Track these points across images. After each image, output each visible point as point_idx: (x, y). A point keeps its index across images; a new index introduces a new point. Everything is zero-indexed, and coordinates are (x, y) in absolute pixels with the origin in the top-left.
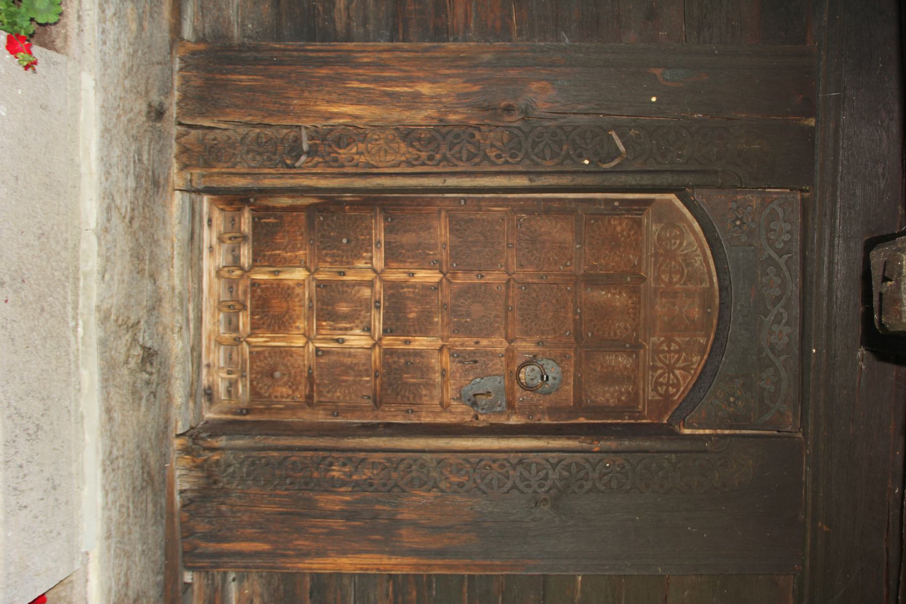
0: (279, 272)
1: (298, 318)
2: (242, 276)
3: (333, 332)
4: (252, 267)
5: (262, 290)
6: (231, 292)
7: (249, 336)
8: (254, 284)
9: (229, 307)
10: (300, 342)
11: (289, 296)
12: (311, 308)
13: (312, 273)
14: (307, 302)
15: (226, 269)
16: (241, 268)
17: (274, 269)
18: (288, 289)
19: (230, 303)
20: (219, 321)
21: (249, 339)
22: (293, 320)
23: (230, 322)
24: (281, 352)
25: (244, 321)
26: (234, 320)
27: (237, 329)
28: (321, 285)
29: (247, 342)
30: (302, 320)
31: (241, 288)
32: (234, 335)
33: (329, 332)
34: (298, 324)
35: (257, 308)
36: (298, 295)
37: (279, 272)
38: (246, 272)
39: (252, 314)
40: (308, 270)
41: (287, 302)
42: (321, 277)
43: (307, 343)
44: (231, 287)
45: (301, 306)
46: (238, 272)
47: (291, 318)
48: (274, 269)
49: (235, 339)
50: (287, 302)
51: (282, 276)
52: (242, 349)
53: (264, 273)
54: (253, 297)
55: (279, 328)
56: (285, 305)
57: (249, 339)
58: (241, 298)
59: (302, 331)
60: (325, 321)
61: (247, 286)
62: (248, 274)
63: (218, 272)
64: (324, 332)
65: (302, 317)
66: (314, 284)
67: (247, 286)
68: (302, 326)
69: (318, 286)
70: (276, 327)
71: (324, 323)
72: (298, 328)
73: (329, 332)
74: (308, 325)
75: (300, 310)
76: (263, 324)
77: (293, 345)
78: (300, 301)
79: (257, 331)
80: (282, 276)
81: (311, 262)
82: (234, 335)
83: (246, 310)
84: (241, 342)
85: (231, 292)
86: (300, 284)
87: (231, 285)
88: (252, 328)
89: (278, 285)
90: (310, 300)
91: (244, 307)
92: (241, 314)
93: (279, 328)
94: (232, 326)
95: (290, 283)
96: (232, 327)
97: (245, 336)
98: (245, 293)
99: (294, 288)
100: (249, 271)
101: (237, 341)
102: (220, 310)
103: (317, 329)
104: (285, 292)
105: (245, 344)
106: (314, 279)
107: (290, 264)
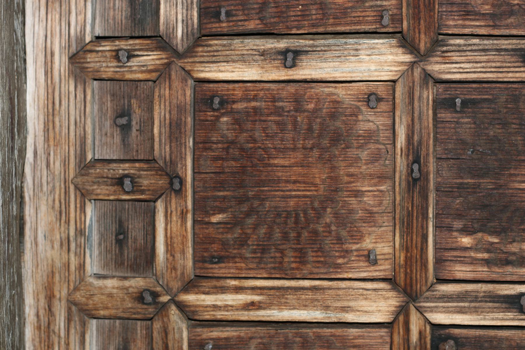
0: (297, 53)
1: (370, 217)
2: (163, 73)
3: (497, 272)
4: (201, 37)
5: (238, 123)
6: (125, 129)
7: (190, 286)
8: (210, 98)
9: (119, 181)
10: (378, 306)
11: (337, 138)
12: (416, 183)
13: (421, 56)
14: (401, 163)
15: (107, 47)
16: (161, 42)
17: (282, 44)
18: (333, 116)
19: (122, 169)
20: (80, 232)
21: (190, 298)
22: (349, 227)
23: (119, 236)
24: (305, 342)
25: (170, 230)
26: (135, 228)
27: (145, 260)
28: (453, 97)
29: (182, 307)
30: (386, 228)
31: (160, 113)
32: (137, 283)
33: (483, 271)
34: (368, 244)
35: (221, 185)
36: (370, 136)
37: (297, 53)
38: (180, 56)
39: (201, 207)
40: (407, 43)
41: (328, 161)
42: (458, 66)
43: (403, 311)
44: (123, 113)
45: (382, 178)
46: (151, 59)
47: (343, 220)
48: (282, 44)
49: (140, 298)
50: (328, 161)
51: (308, 70)
52: (165, 332)
53: (243, 59)
54: (202, 146)
55: (302, 259)
56: (319, 174)
57: (190, 298)
58: (161, 149)
59: (384, 268)
60: (466, 231)
61: (181, 109)
62: (187, 63)
63: (77, 58)
64: (461, 271)
65: (386, 221)
66: (429, 94)
67: (181, 109)
68: (383, 248)
69: (440, 104)
70: (290, 257)
71: (466, 241)
72: (370, 258)
73: (483, 271)
74: (406, 248)
75: (374, 194)
76: (242, 242)
77: (350, 317)
78: (375, 158)
79: (218, 270)
80: (308, 70)
81: (416, 17)
82: (137, 283)
83: (180, 192)
84: (164, 306)
85: (125, 129)
86: (372, 96)
87: (126, 104)
88: (199, 260)
89: (298, 101)
90: (415, 155)
91: (174, 184)
92: (160, 206)
93: (302, 259)
94: (129, 250)
95: (341, 92)
96: (129, 253)
97: (176, 285)
98: (175, 130)
99: (355, 113)
100: (190, 52)
101: (150, 304)
102: (84, 195)
103: (439, 262)
104: (326, 125)
105: (173, 311)
106: (428, 77)
107: (339, 28)
